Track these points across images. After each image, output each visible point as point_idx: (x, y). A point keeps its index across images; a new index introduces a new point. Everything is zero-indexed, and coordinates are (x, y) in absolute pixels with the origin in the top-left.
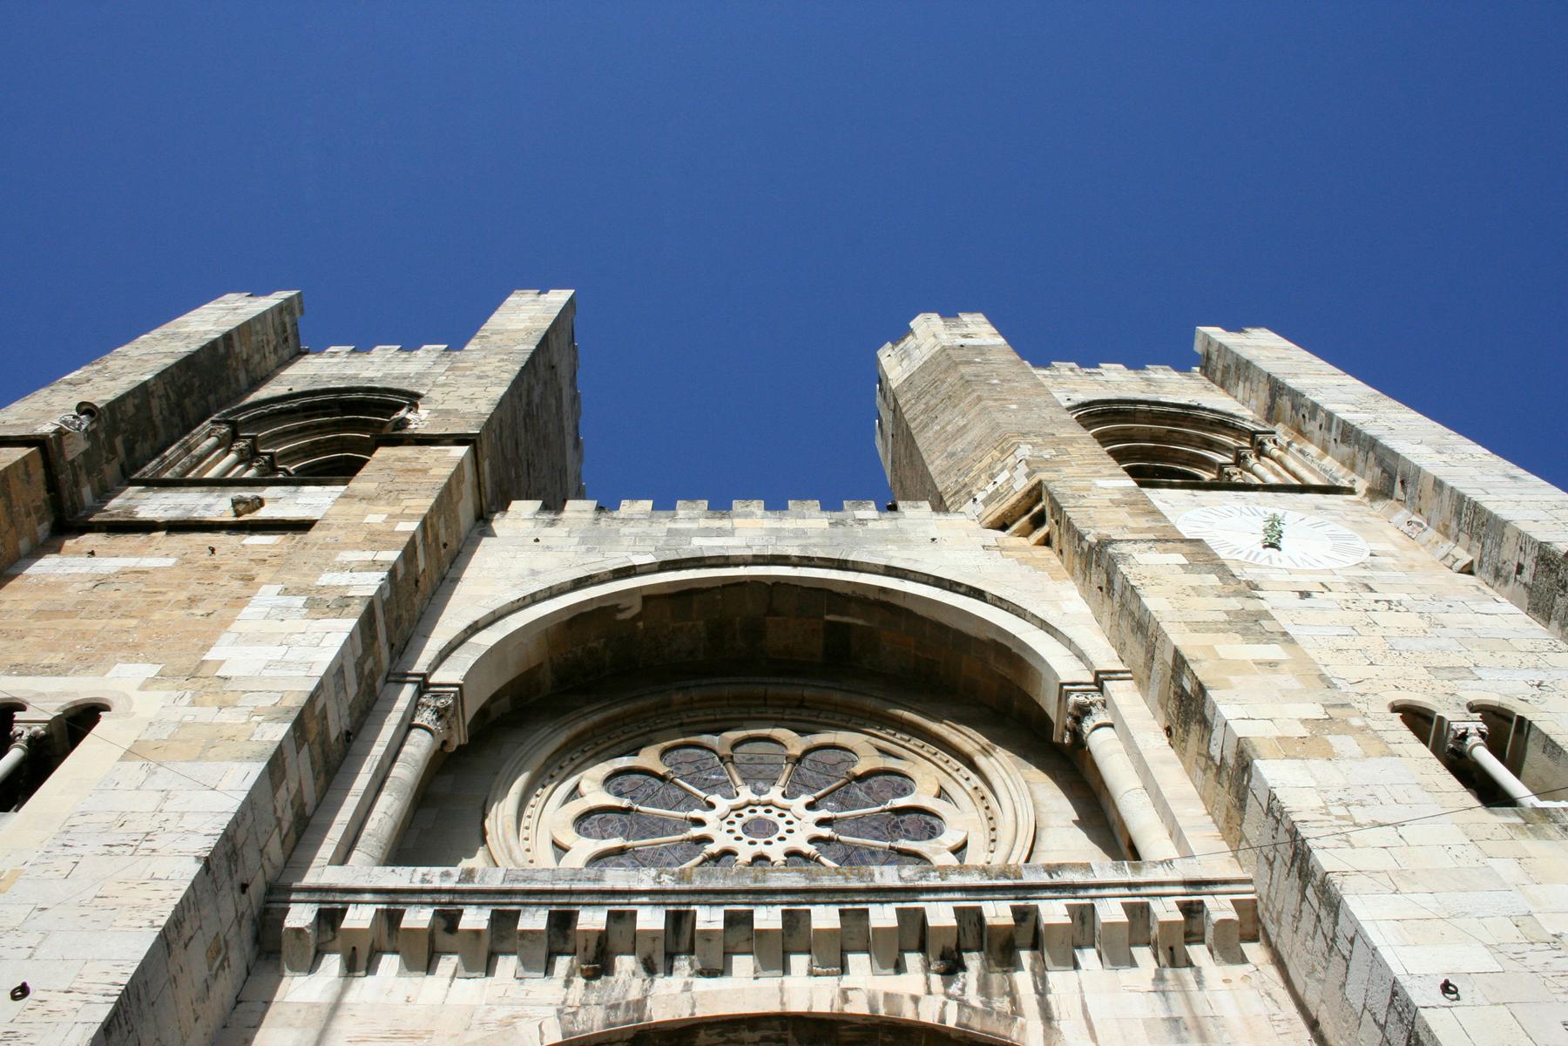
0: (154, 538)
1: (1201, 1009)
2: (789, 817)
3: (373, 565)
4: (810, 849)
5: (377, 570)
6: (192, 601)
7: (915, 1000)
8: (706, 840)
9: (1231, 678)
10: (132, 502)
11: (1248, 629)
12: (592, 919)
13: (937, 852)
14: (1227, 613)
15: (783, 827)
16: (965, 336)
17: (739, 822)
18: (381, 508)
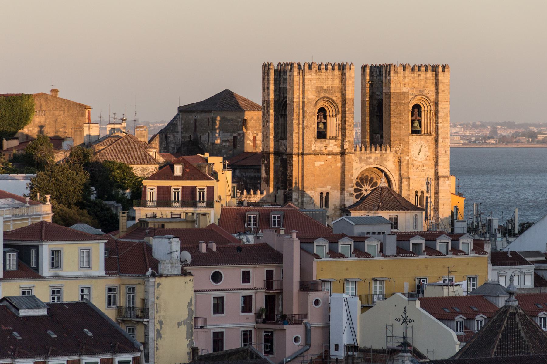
8: (363, 193)
16: (404, 86)
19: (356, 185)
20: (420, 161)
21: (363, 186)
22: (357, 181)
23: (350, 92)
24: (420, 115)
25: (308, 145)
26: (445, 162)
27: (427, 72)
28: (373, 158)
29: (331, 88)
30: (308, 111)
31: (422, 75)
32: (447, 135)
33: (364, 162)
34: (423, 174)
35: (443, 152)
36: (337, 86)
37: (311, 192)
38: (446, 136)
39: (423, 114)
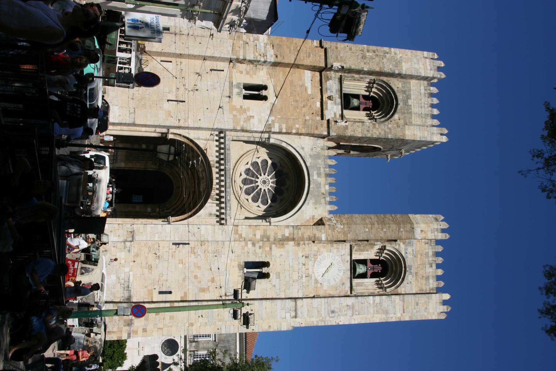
1: (212, 217)
2: (266, 186)
3: (281, 129)
4: (259, 188)
5: (279, 130)
6: (296, 101)
8: (261, 175)
9: (251, 230)
10: (333, 78)
11: (264, 236)
12: (222, 162)
14: (269, 235)
15: (264, 185)
16: (422, 231)
17: (266, 180)
18: (301, 126)
21: (270, 177)
22: (278, 164)
24: (373, 276)
25: (339, 57)
26: (318, 311)
27: (435, 279)
28: (319, 180)
29: (410, 112)
30: (385, 60)
31: (431, 270)
32: (357, 313)
34: (295, 277)
35: (332, 305)
36: (413, 122)
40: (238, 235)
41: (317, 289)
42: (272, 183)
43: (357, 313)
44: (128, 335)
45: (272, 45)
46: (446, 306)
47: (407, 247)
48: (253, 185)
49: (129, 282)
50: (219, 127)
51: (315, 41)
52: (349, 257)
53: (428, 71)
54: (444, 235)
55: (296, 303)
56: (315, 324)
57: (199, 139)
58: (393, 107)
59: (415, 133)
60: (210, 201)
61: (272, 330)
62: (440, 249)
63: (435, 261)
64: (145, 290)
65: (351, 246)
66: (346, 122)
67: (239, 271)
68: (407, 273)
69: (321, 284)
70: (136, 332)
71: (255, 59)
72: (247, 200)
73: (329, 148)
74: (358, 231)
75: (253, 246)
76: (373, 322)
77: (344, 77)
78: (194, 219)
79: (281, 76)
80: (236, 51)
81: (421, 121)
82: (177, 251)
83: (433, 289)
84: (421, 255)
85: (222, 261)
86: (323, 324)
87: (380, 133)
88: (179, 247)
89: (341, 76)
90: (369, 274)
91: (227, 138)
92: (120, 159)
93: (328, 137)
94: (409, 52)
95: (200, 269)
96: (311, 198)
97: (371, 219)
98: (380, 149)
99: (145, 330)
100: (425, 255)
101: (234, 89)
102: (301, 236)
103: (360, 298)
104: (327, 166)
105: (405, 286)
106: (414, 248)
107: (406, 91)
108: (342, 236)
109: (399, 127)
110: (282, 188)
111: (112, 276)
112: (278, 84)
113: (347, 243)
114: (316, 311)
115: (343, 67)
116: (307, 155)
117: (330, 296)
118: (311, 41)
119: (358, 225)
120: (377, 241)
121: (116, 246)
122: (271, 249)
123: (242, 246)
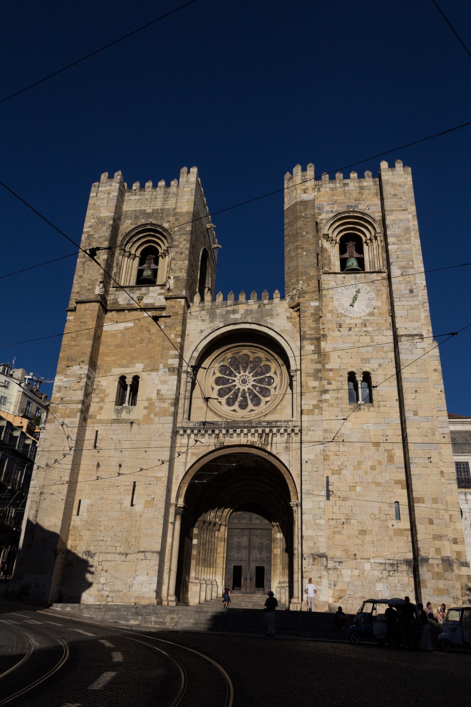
0: (126, 314)
6: (142, 341)
7: (256, 442)
12: (217, 432)
13: (272, 389)
14: (314, 369)
15: (248, 381)
16: (305, 192)
17: (241, 380)
18: (173, 331)
19: (221, 372)
20: (356, 316)
21: (237, 374)
22: (222, 364)
23: (185, 204)
24: (360, 250)
25: (88, 287)
26: (412, 309)
27: (363, 180)
30: (96, 236)
33: (220, 320)
34: (366, 340)
35: (402, 293)
36: (173, 207)
37: (81, 368)
38: (408, 264)
39: (365, 247)
40: (315, 410)
41: (381, 313)
42: (245, 372)
43: (411, 263)
44: (464, 566)
45: (67, 368)
46: (396, 165)
47: (324, 210)
48: (247, 395)
49: (385, 563)
50: (170, 435)
51: (68, 318)
52: (338, 276)
53: (113, 188)
54: (308, 168)
55: (402, 336)
56: (428, 314)
57: (185, 463)
58: (154, 229)
59: (186, 201)
60: (268, 449)
61: (440, 368)
62: (326, 177)
63: (340, 180)
64: (395, 539)
65: (324, 273)
66: (169, 278)
67: (363, 410)
68: (356, 210)
69: (374, 308)
70: (459, 554)
71: (84, 388)
72: (267, 402)
73: (202, 299)
74: (306, 264)
75: (328, 393)
76: (420, 245)
77: (115, 285)
78: (294, 470)
79: (109, 359)
80: (71, 413)
81: (172, 199)
82: (338, 494)
83: (375, 182)
84: (334, 195)
85: (349, 432)
86: (427, 305)
87: (185, 240)
88: (333, 491)
89: (113, 287)
90: (359, 256)
91: (185, 425)
92: (211, 575)
93: (189, 301)
94: (89, 212)
95: (362, 462)
96: (265, 321)
97: (290, 250)
98: (205, 250)
99: (455, 541)
100: (333, 191)
101: (122, 418)
102: (314, 331)
103: (391, 260)
104: (225, 302)
105: (372, 212)
106: (325, 204)
107: (135, 215)
108: (313, 281)
109: (178, 218)
110: (251, 360)
111: (377, 589)
112: (119, 362)
113: (321, 278)
114: (411, 311)
115: (101, 282)
116: (210, 326)
117: (389, 297)
118: (67, 324)
119: (299, 264)
120: (318, 243)
121: (334, 582)
122: (331, 370)
123: (329, 407)
